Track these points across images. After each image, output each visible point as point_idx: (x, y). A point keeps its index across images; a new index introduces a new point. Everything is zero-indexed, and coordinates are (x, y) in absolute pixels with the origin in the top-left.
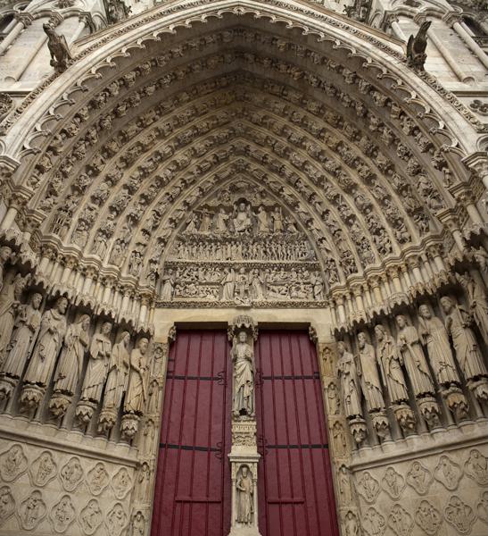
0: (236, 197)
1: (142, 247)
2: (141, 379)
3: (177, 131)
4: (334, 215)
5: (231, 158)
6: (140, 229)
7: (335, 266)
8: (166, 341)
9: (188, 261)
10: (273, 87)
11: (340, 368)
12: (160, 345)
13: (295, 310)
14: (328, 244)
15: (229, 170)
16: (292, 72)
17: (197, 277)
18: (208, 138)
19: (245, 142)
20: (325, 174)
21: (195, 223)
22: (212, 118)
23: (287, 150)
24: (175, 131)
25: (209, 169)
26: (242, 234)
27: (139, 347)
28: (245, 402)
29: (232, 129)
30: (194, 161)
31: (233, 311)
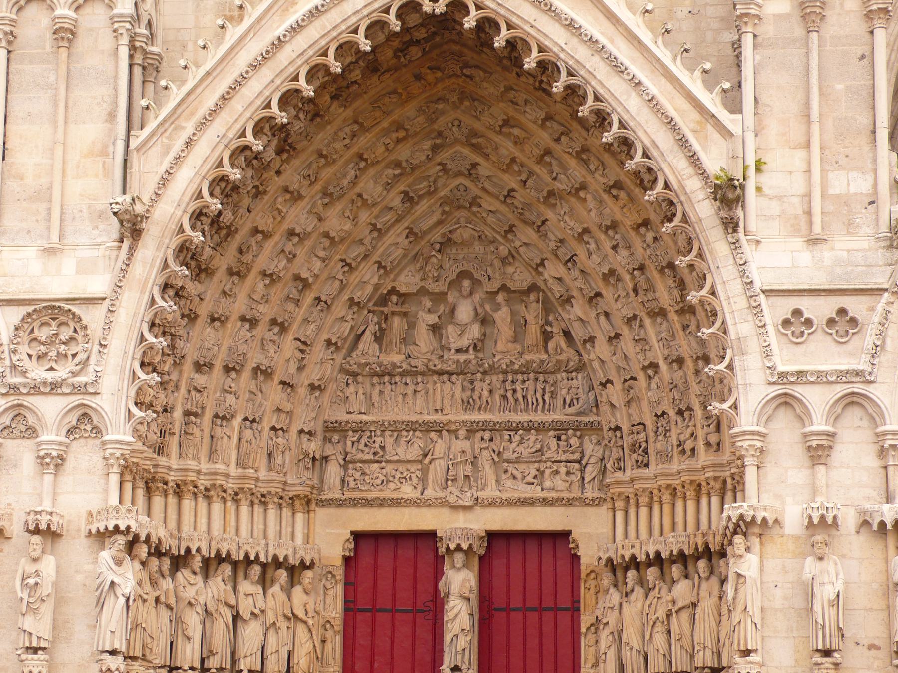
2: (310, 630)
3: (327, 173)
4: (627, 345)
6: (276, 380)
7: (622, 437)
8: (339, 562)
9: (364, 418)
11: (598, 613)
12: (330, 569)
13: (548, 510)
14: (615, 393)
17: (383, 448)
18: (387, 167)
22: (399, 126)
23: (551, 194)
25: (397, 221)
26: (462, 358)
27: (300, 583)
28: (459, 657)
29: (440, 134)
30: (364, 216)
31: (445, 512)
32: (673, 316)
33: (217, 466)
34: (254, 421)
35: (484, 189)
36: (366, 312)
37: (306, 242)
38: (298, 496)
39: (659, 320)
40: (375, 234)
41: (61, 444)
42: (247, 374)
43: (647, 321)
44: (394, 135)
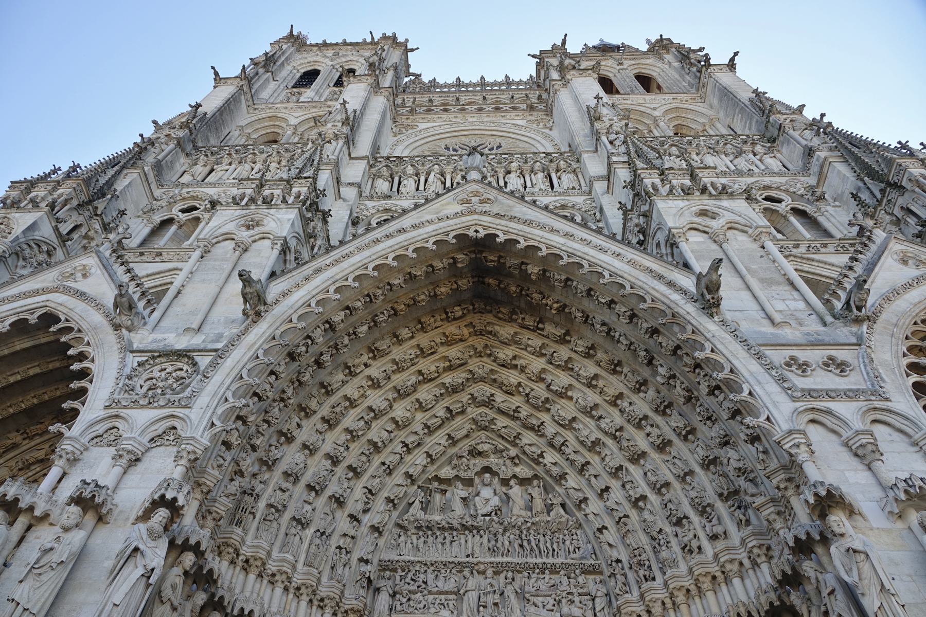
0: (478, 463)
1: (349, 540)
5: (469, 409)
6: (346, 514)
10: (523, 319)
15: (467, 427)
16: (549, 303)
18: (436, 387)
19: (488, 390)
20: (600, 436)
21: (422, 502)
24: (394, 377)
30: (419, 416)
32: (654, 455)
33: (286, 555)
34: (323, 534)
35: (501, 412)
36: (416, 487)
37: (379, 421)
38: (352, 609)
39: (642, 462)
40: (426, 431)
41: (140, 443)
42: (323, 499)
43: (631, 468)
44: (442, 365)
